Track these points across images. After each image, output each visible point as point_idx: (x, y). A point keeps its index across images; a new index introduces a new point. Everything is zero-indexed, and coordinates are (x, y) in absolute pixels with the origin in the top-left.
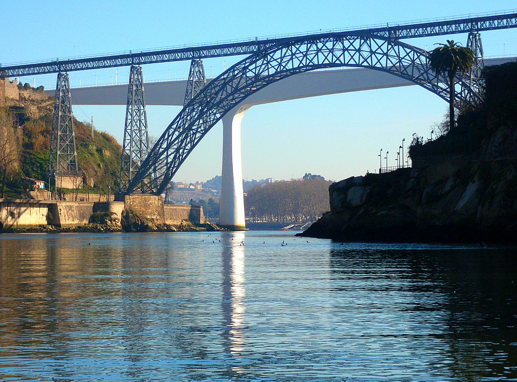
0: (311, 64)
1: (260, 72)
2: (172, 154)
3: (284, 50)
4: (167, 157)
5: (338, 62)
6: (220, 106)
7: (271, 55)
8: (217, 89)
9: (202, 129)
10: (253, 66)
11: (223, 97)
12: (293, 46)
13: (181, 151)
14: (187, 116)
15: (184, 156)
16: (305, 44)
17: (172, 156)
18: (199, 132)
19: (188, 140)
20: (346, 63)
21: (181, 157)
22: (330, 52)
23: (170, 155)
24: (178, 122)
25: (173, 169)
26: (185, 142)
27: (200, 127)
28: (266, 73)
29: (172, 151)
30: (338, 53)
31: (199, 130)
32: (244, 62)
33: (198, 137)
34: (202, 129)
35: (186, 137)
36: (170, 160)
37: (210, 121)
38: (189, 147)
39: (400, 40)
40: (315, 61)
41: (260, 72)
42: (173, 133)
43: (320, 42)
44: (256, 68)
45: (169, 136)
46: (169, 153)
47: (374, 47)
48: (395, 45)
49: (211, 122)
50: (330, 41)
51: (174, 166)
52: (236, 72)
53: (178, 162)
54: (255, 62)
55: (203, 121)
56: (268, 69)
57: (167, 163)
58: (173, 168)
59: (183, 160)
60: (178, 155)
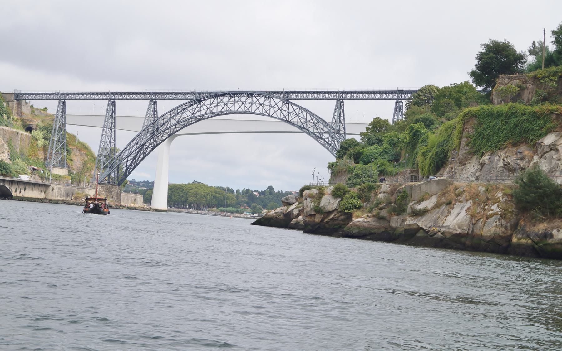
0: (229, 110)
1: (195, 112)
2: (130, 160)
3: (213, 99)
4: (127, 161)
5: (247, 111)
6: (166, 132)
7: (203, 102)
8: (165, 121)
9: (152, 145)
10: (191, 108)
11: (169, 125)
12: (218, 98)
13: (137, 159)
14: (144, 136)
16: (226, 97)
17: (130, 162)
18: (150, 147)
19: (142, 152)
20: (253, 111)
22: (243, 103)
23: (129, 160)
24: (137, 139)
25: (129, 170)
27: (151, 144)
28: (198, 114)
30: (248, 105)
31: (150, 146)
34: (152, 145)
36: (129, 164)
38: (142, 156)
39: (290, 101)
40: (232, 109)
41: (195, 112)
43: (237, 97)
44: (193, 109)
45: (130, 148)
46: (129, 159)
47: (273, 104)
48: (287, 103)
50: (244, 97)
52: (179, 111)
54: (192, 105)
55: (154, 140)
56: (200, 111)
57: (126, 166)
59: (137, 165)
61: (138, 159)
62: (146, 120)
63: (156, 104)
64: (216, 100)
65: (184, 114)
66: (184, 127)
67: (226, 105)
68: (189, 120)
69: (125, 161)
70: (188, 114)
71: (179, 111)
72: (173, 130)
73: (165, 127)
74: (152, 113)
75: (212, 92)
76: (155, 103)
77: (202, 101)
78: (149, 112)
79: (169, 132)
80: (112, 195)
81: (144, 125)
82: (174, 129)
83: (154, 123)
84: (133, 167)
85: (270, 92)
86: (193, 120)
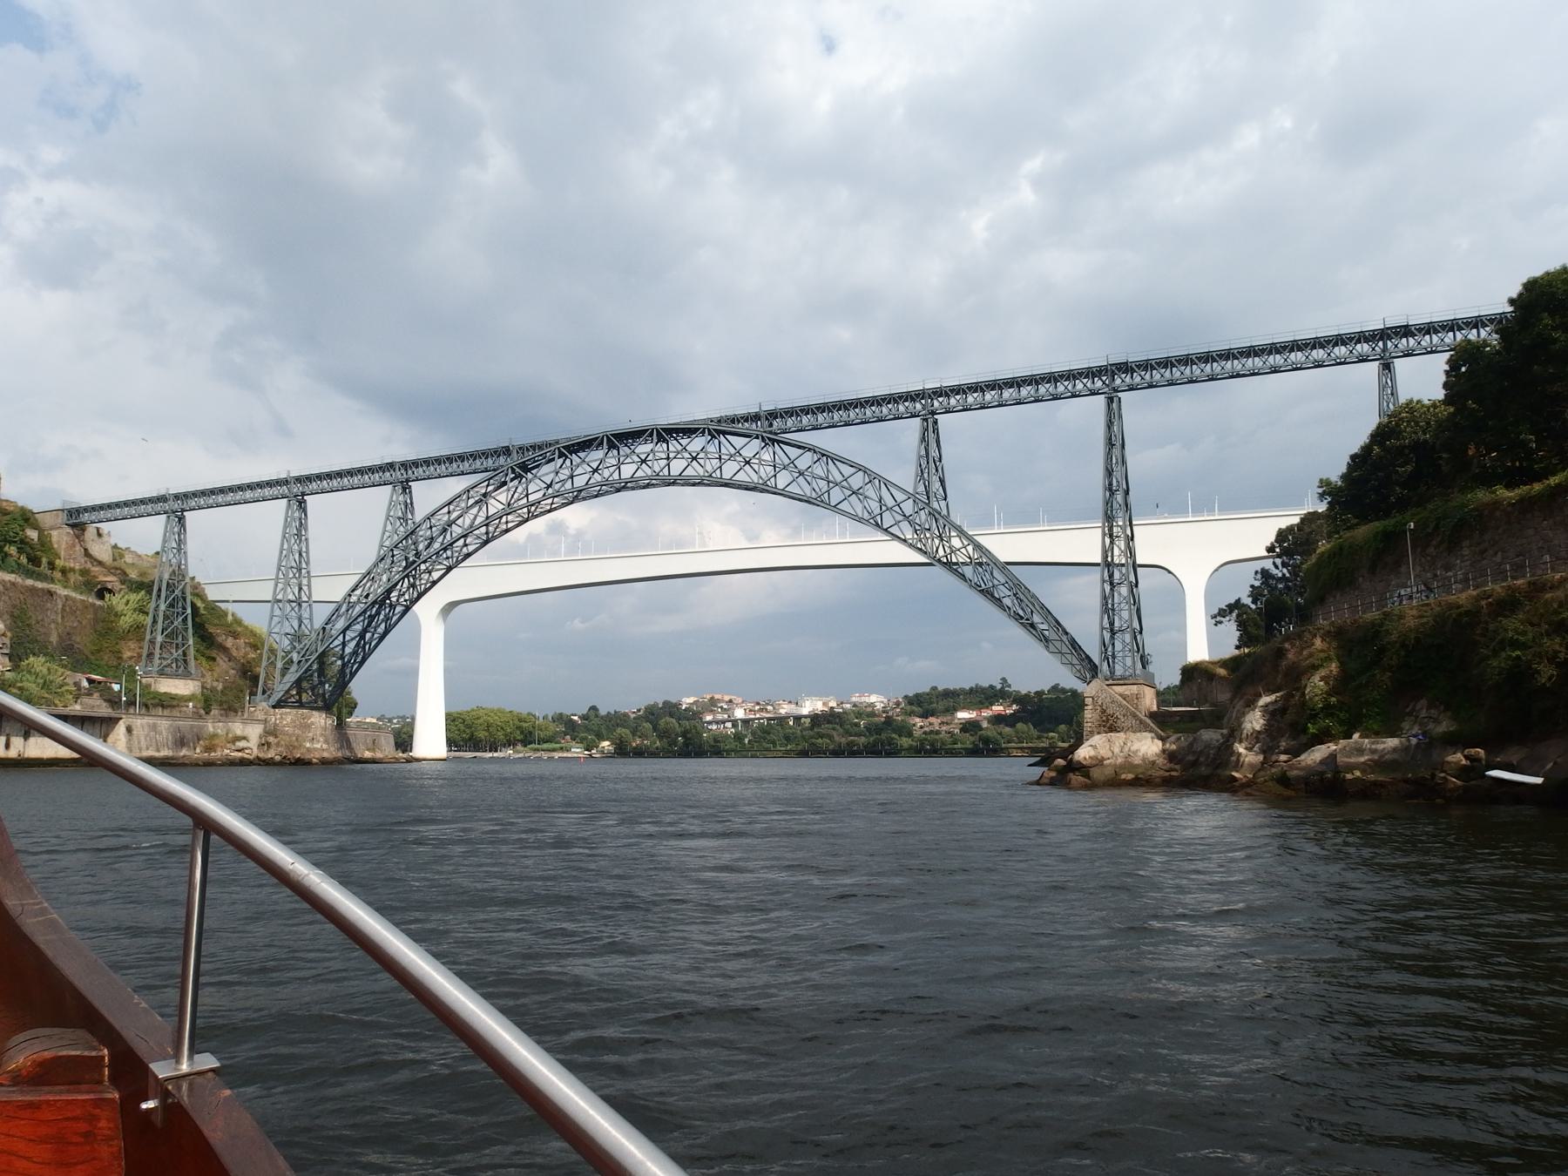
2: (353, 639)
4: (344, 644)
13: (368, 635)
15: (373, 644)
17: (353, 644)
21: (367, 647)
24: (365, 585)
25: (352, 667)
27: (403, 595)
29: (353, 635)
32: (486, 483)
34: (407, 597)
35: (378, 613)
36: (348, 650)
37: (420, 585)
38: (381, 629)
46: (347, 638)
54: (505, 483)
56: (527, 495)
58: (354, 664)
59: (372, 651)
62: (387, 534)
63: (410, 492)
64: (568, 462)
65: (484, 508)
66: (486, 542)
67: (595, 471)
68: (501, 518)
69: (337, 642)
70: (494, 506)
71: (471, 501)
73: (436, 545)
74: (400, 514)
75: (557, 443)
76: (406, 489)
78: (392, 514)
79: (448, 558)
80: (310, 734)
83: (406, 538)
86: (510, 517)
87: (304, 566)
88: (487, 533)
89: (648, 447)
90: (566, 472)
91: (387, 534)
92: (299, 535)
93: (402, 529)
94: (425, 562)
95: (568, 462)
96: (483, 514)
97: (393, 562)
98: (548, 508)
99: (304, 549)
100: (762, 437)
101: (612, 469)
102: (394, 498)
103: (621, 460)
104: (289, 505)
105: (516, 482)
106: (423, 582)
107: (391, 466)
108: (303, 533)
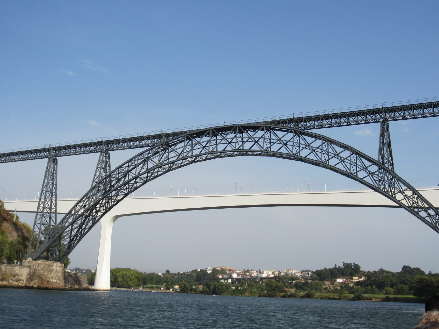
2: (76, 228)
4: (72, 230)
7: (172, 147)
13: (84, 226)
17: (75, 231)
24: (84, 201)
26: (88, 219)
33: (100, 216)
36: (73, 233)
37: (111, 202)
42: (79, 210)
46: (74, 227)
49: (112, 203)
51: (76, 239)
53: (80, 236)
59: (84, 234)
60: (80, 230)
61: (85, 228)
62: (97, 176)
64: (190, 142)
68: (154, 169)
69: (68, 229)
72: (132, 186)
73: (121, 183)
75: (185, 132)
76: (107, 155)
77: (170, 146)
78: (100, 166)
79: (126, 189)
81: (93, 181)
82: (134, 184)
83: (105, 179)
84: (78, 238)
85: (272, 122)
87: (54, 191)
88: (147, 177)
89: (233, 136)
90: (189, 148)
91: (97, 176)
92: (53, 176)
93: (104, 174)
94: (115, 190)
95: (190, 142)
96: (145, 168)
97: (98, 190)
98: (179, 165)
99: (55, 183)
100: (295, 131)
101: (214, 146)
102: (101, 158)
103: (218, 141)
104: (49, 162)
105: (163, 152)
106: (113, 200)
107: (100, 143)
108: (55, 175)
